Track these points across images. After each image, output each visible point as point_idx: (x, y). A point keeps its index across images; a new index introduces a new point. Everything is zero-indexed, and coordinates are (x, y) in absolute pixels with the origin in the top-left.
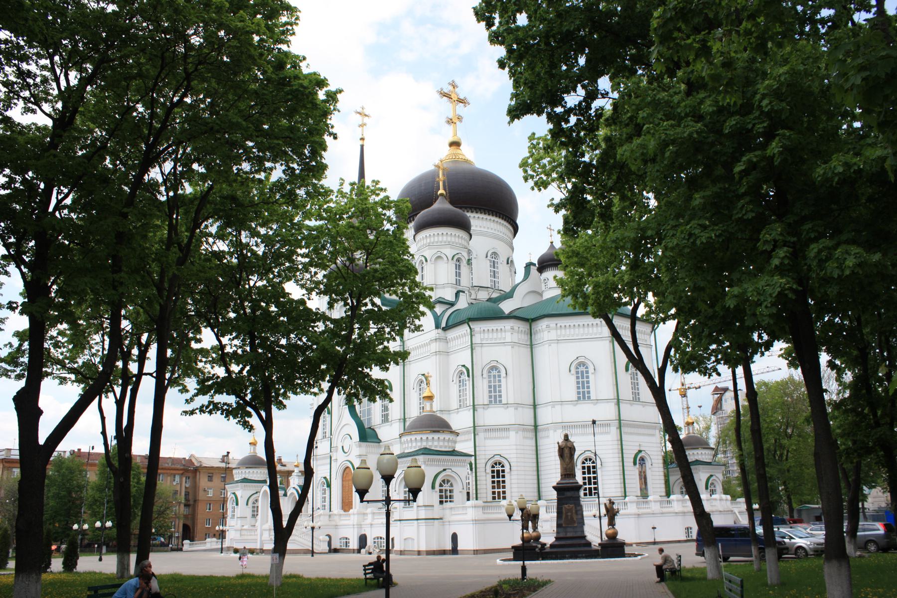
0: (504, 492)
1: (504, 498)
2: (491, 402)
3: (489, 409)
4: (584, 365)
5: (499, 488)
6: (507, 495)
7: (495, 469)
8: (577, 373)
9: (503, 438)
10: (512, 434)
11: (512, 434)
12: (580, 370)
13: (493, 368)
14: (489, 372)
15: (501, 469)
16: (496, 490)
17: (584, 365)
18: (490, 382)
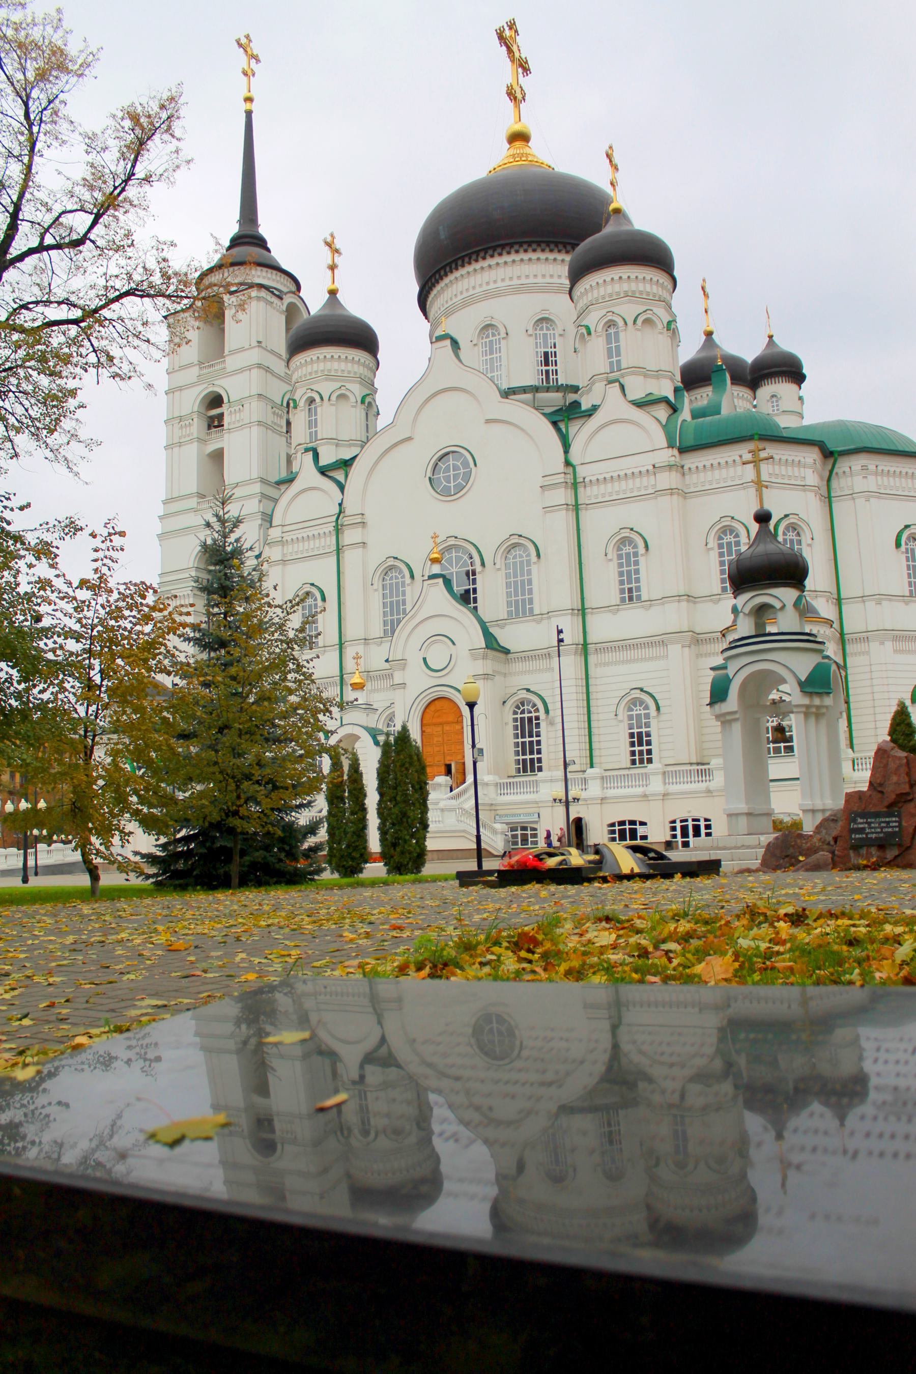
0: (649, 752)
1: (650, 761)
2: (623, 600)
3: (620, 613)
4: (731, 532)
5: (640, 744)
6: (654, 756)
7: (634, 713)
8: (720, 546)
9: (656, 658)
10: (675, 650)
11: (675, 650)
12: (725, 541)
13: (625, 541)
14: (619, 549)
15: (643, 712)
16: (637, 748)
17: (731, 532)
18: (620, 565)
